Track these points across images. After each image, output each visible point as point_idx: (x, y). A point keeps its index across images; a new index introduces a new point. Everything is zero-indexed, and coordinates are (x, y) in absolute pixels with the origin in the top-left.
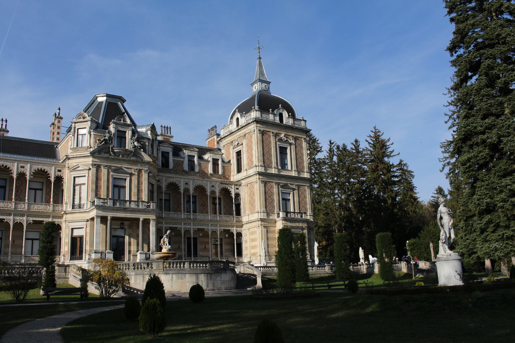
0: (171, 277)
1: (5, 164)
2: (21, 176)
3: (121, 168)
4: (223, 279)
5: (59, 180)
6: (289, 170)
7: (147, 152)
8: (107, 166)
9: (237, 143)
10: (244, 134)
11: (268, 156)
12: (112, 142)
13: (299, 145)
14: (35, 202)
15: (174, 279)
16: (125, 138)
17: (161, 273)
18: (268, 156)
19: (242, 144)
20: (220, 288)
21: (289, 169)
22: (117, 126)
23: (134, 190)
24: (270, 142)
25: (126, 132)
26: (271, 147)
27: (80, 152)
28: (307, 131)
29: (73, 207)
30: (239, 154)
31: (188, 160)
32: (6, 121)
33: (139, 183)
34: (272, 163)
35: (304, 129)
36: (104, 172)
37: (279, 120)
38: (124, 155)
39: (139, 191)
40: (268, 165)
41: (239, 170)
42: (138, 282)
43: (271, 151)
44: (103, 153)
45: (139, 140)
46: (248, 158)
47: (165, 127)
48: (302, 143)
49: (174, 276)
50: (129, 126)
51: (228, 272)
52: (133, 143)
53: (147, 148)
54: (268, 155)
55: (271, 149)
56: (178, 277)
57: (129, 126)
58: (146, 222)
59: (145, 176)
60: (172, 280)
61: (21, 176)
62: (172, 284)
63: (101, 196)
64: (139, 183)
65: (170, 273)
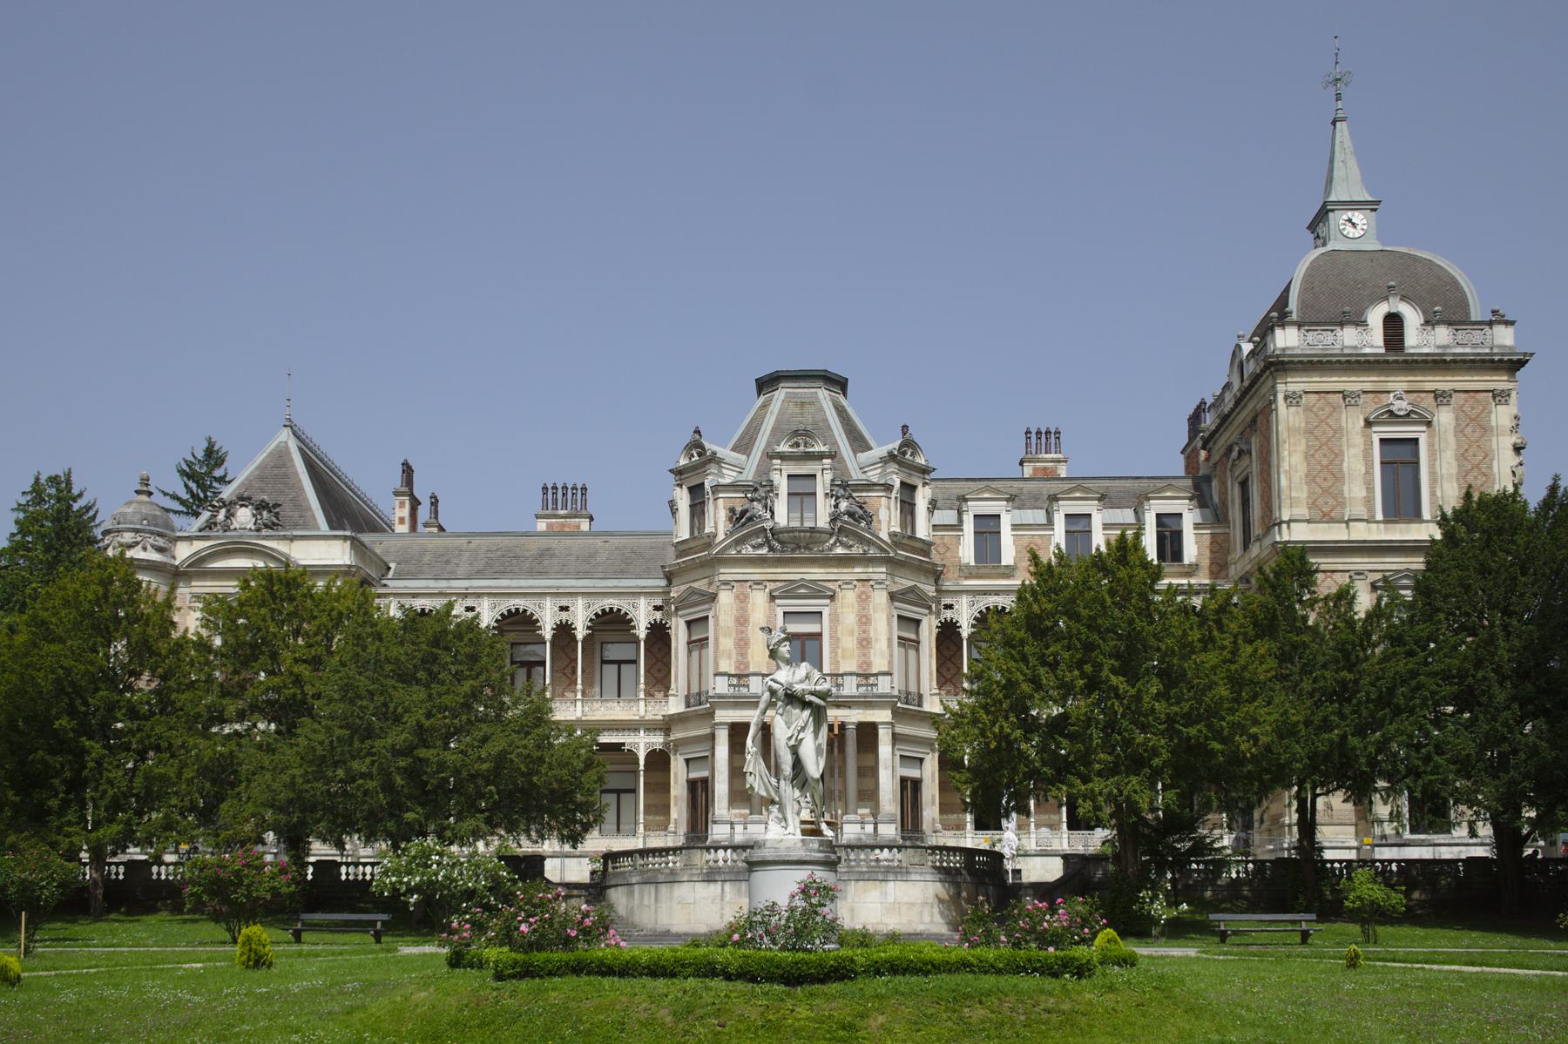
0: (720, 891)
1: (521, 603)
2: (564, 631)
3: (803, 584)
4: (891, 899)
5: (659, 634)
6: (1428, 522)
7: (884, 526)
8: (758, 583)
9: (1237, 448)
10: (1249, 419)
11: (1325, 479)
12: (772, 512)
13: (1472, 420)
14: (619, 696)
15: (728, 897)
16: (815, 494)
17: (695, 879)
18: (1325, 479)
19: (1250, 453)
20: (877, 923)
21: (1425, 518)
22: (785, 463)
23: (849, 642)
24: (1338, 431)
25: (815, 476)
26: (1341, 445)
27: (696, 553)
28: (1510, 361)
29: (688, 705)
30: (1244, 485)
31: (1066, 532)
32: (584, 489)
33: (864, 620)
34: (1342, 504)
35: (1496, 358)
36: (759, 598)
37: (1381, 343)
38: (811, 546)
39: (865, 643)
40: (1324, 515)
41: (1246, 545)
42: (646, 902)
43: (1343, 460)
44: (750, 549)
45: (854, 495)
46: (1262, 499)
47: (1048, 432)
48: (1491, 412)
49: (728, 886)
50: (820, 457)
51: (917, 877)
52: (836, 506)
53: (883, 514)
54: (1329, 477)
55: (1342, 452)
56: (739, 891)
57: (820, 457)
58: (868, 733)
59: (880, 598)
60: (722, 899)
61: (564, 631)
62: (722, 909)
63: (747, 666)
64: (864, 620)
65: (717, 878)
